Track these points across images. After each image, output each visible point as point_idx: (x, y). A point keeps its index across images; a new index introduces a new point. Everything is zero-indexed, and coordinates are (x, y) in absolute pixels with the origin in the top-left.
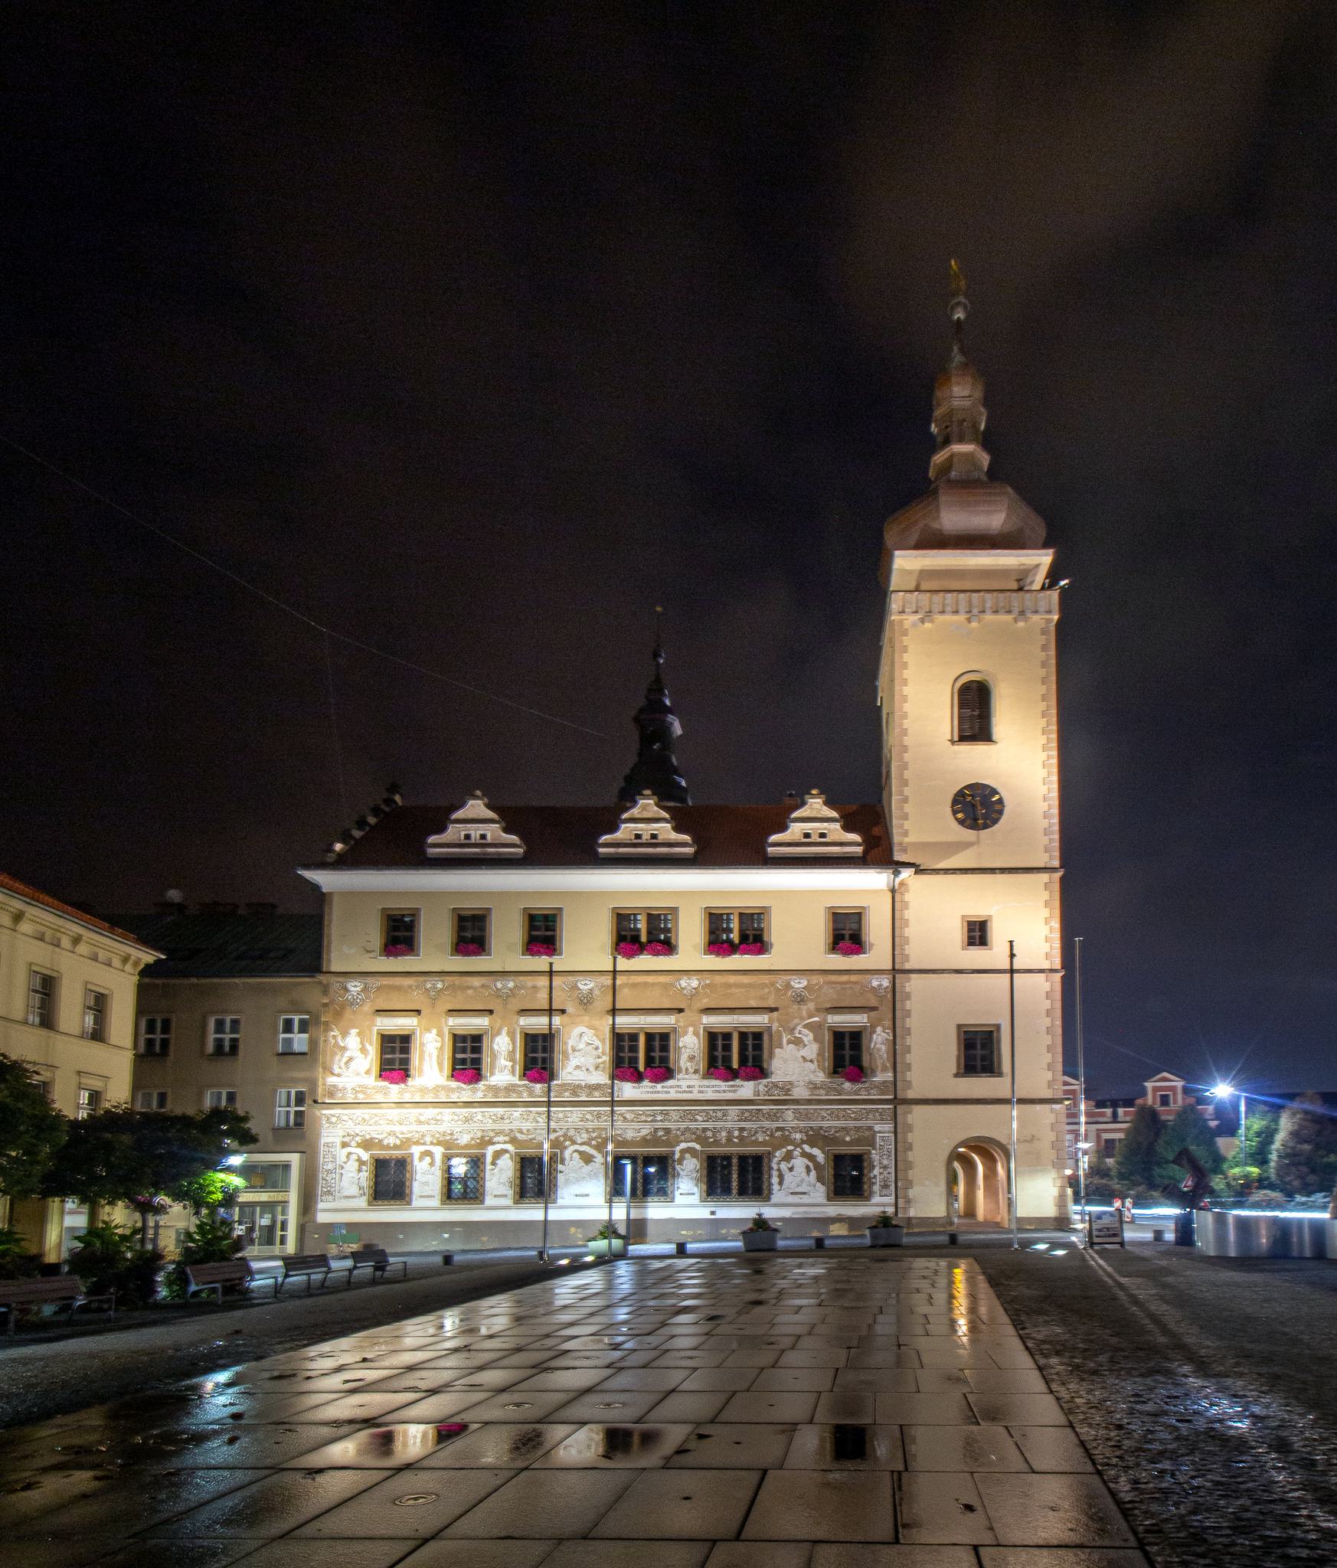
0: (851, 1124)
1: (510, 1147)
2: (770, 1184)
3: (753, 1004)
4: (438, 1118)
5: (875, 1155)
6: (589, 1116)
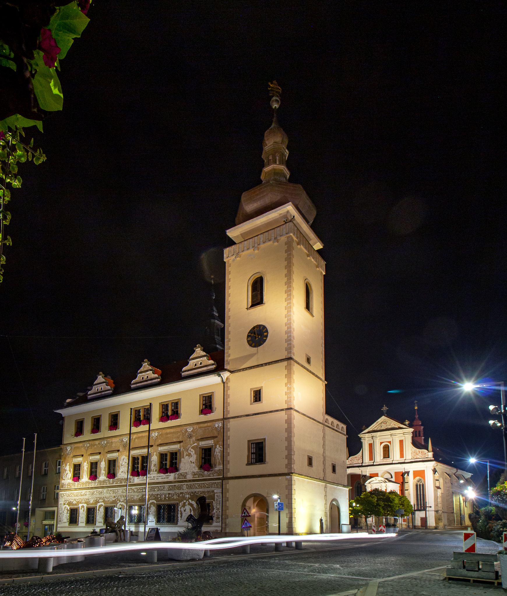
0: (206, 490)
1: (103, 504)
2: (178, 517)
3: (175, 440)
4: (86, 493)
6: (124, 491)
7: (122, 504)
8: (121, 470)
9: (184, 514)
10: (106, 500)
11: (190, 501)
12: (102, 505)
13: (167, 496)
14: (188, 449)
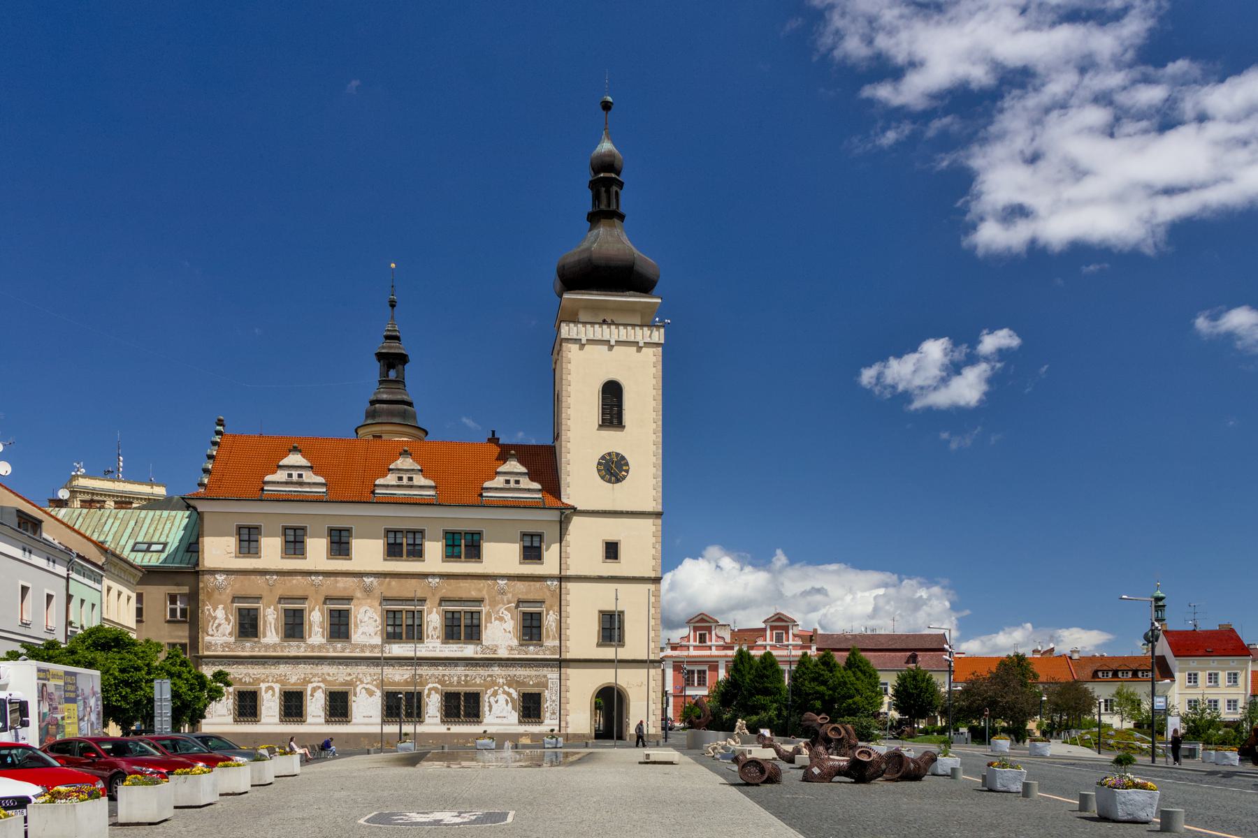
1: (322, 685)
5: (547, 694)
7: (367, 686)
8: (360, 630)
9: (495, 706)
10: (329, 678)
11: (506, 688)
12: (320, 687)
13: (463, 678)
14: (499, 611)
